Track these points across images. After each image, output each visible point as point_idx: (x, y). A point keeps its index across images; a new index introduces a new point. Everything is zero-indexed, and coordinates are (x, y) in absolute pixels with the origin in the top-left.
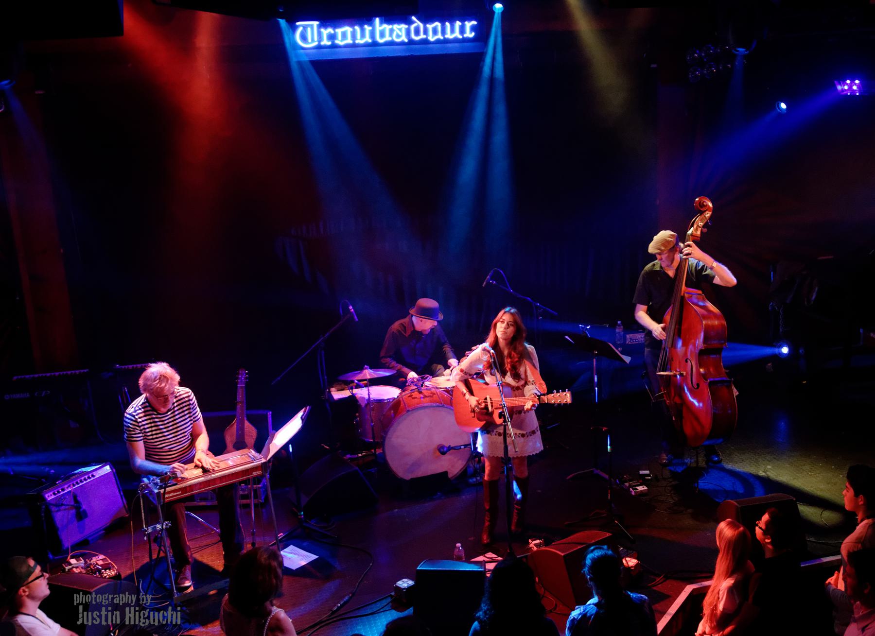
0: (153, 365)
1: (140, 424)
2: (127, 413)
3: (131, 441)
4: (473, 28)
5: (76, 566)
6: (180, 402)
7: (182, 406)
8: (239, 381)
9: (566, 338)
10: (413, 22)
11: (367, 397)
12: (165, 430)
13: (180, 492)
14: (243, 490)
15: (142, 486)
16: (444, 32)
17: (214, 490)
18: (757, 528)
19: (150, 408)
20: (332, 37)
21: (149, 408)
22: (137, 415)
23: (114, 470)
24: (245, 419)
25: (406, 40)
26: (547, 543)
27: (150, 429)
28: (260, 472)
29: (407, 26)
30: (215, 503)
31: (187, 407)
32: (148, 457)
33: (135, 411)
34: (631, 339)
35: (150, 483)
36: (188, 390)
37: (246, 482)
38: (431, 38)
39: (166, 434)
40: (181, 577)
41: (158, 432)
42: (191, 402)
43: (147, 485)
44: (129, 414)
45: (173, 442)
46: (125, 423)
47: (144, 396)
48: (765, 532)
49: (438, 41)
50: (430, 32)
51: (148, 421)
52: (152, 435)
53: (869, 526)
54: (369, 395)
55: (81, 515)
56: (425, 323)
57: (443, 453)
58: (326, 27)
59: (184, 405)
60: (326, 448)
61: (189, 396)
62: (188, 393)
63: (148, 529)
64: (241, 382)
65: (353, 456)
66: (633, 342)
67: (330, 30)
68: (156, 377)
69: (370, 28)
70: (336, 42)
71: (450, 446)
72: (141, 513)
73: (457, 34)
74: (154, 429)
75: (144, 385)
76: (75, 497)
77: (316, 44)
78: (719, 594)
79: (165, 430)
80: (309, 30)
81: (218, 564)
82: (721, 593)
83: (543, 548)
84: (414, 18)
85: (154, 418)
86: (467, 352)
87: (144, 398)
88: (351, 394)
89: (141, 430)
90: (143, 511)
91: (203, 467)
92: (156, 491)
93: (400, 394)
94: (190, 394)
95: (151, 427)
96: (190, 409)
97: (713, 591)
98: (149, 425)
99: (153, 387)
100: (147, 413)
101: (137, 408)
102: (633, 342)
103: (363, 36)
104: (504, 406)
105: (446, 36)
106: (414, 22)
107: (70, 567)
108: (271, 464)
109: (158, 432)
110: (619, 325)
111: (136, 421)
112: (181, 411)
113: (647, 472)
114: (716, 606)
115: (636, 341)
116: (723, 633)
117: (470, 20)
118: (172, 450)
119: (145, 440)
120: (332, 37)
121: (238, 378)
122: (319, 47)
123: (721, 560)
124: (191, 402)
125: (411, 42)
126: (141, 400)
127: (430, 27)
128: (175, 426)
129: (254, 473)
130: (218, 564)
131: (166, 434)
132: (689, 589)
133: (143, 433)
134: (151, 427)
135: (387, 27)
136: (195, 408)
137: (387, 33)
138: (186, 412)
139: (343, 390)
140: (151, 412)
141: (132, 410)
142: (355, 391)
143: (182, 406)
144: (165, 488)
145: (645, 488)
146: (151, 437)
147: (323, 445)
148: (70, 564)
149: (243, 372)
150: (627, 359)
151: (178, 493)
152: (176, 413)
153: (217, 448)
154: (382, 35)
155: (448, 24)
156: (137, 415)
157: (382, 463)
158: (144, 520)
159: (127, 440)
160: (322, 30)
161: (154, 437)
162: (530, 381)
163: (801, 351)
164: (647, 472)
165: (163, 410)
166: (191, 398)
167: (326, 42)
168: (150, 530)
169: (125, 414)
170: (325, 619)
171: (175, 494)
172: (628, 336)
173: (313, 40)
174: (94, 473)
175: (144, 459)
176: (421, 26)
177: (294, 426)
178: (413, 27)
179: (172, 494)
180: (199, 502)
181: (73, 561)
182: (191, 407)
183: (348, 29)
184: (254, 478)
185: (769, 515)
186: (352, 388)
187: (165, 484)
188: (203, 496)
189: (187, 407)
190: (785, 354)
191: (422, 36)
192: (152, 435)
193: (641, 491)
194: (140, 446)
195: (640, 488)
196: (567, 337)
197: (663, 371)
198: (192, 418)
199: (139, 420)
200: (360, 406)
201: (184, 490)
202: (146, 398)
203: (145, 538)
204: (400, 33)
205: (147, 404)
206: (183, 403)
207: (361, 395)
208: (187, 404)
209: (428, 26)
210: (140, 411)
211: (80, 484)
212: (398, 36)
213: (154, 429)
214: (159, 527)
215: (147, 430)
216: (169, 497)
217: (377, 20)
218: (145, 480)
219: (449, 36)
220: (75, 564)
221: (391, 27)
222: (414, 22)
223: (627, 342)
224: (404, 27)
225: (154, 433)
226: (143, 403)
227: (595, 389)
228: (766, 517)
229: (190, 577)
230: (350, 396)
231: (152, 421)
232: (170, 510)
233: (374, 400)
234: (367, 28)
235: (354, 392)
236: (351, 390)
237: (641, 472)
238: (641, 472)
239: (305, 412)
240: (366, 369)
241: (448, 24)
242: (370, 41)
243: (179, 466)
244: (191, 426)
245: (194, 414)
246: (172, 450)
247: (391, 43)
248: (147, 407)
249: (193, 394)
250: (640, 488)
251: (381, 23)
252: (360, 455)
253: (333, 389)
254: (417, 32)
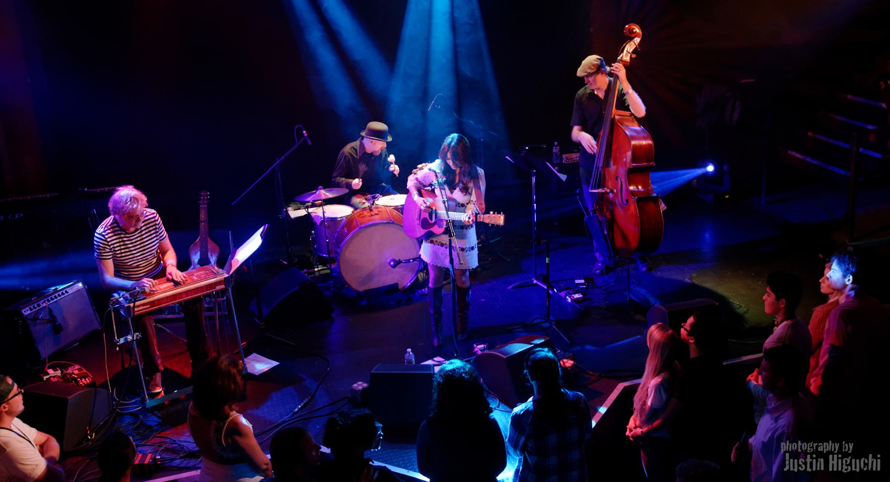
0: (121, 188)
1: (110, 243)
2: (97, 233)
3: (100, 259)
5: (53, 375)
6: (146, 223)
7: (148, 226)
8: (201, 202)
9: (507, 159)
11: (321, 215)
12: (133, 249)
13: (149, 306)
14: (208, 303)
15: (112, 300)
17: (180, 303)
18: (682, 330)
19: (118, 228)
21: (117, 229)
22: (106, 235)
23: (86, 287)
24: (208, 238)
26: (489, 348)
27: (119, 248)
28: (223, 286)
30: (182, 315)
31: (154, 227)
32: (117, 274)
33: (104, 232)
34: (567, 159)
35: (120, 298)
36: (153, 211)
37: (208, 295)
39: (134, 252)
40: (152, 384)
41: (127, 250)
42: (157, 223)
43: (117, 300)
44: (99, 234)
45: (140, 260)
46: (95, 243)
47: (112, 217)
48: (690, 333)
51: (117, 241)
52: (121, 253)
53: (789, 327)
54: (324, 215)
55: (57, 329)
56: (375, 144)
57: (394, 267)
59: (151, 225)
60: (285, 264)
61: (155, 217)
62: (153, 214)
63: (120, 340)
64: (204, 204)
65: (310, 271)
66: (569, 161)
68: (127, 200)
71: (400, 260)
72: (113, 325)
74: (122, 247)
75: (114, 207)
76: (50, 311)
78: (647, 391)
79: (133, 249)
81: (187, 371)
82: (649, 390)
83: (486, 352)
85: (123, 238)
86: (414, 170)
87: (112, 219)
88: (307, 213)
89: (111, 249)
90: (114, 324)
91: (173, 280)
92: (126, 305)
93: (352, 212)
94: (155, 215)
95: (120, 246)
96: (156, 229)
97: (642, 388)
98: (118, 244)
99: (126, 209)
100: (116, 233)
101: (106, 229)
102: (569, 161)
104: (450, 222)
107: (48, 377)
108: (233, 279)
109: (127, 250)
110: (556, 146)
111: (106, 241)
112: (147, 230)
113: (583, 281)
114: (645, 403)
115: (571, 161)
116: (652, 426)
118: (140, 266)
119: (115, 258)
121: (200, 200)
123: (651, 358)
124: (157, 223)
126: (109, 220)
128: (142, 245)
129: (217, 287)
130: (187, 371)
131: (134, 252)
132: (621, 386)
133: (112, 252)
134: (120, 246)
136: (161, 227)
138: (152, 232)
139: (299, 209)
140: (119, 232)
141: (102, 230)
142: (310, 210)
143: (148, 226)
144: (134, 302)
145: (581, 296)
146: (120, 255)
147: (281, 260)
148: (48, 374)
149: (205, 194)
150: (563, 177)
151: (147, 307)
152: (144, 232)
153: (183, 264)
156: (106, 235)
157: (336, 278)
158: (115, 332)
159: (97, 258)
161: (123, 255)
162: (472, 201)
163: (725, 168)
164: (583, 281)
165: (132, 229)
166: (156, 218)
168: (122, 341)
169: (96, 234)
170: (287, 420)
171: (144, 307)
172: (564, 156)
174: (67, 290)
175: (113, 275)
177: (255, 243)
179: (141, 308)
180: (166, 315)
181: (51, 371)
182: (158, 226)
184: (217, 292)
185: (694, 319)
186: (307, 207)
187: (135, 299)
188: (170, 309)
189: (154, 227)
190: (712, 172)
192: (121, 253)
193: (577, 298)
194: (109, 265)
195: (577, 296)
196: (507, 157)
197: (594, 189)
198: (158, 237)
199: (109, 240)
200: (315, 223)
201: (152, 303)
202: (115, 219)
203: (117, 349)
205: (115, 225)
206: (150, 223)
207: (316, 213)
208: (152, 224)
210: (109, 231)
211: (55, 300)
213: (122, 247)
214: (130, 338)
215: (117, 249)
216: (138, 311)
218: (116, 295)
220: (53, 373)
223: (564, 161)
225: (123, 251)
226: (112, 224)
227: (534, 206)
228: (691, 320)
229: (161, 385)
230: (306, 215)
231: (120, 240)
232: (139, 322)
233: (328, 218)
235: (309, 211)
236: (306, 209)
237: (577, 281)
238: (577, 281)
239: (265, 227)
240: (321, 189)
243: (148, 281)
244: (158, 244)
245: (160, 234)
246: (140, 266)
248: (115, 227)
249: (158, 215)
250: (577, 296)
252: (316, 269)
253: (290, 209)
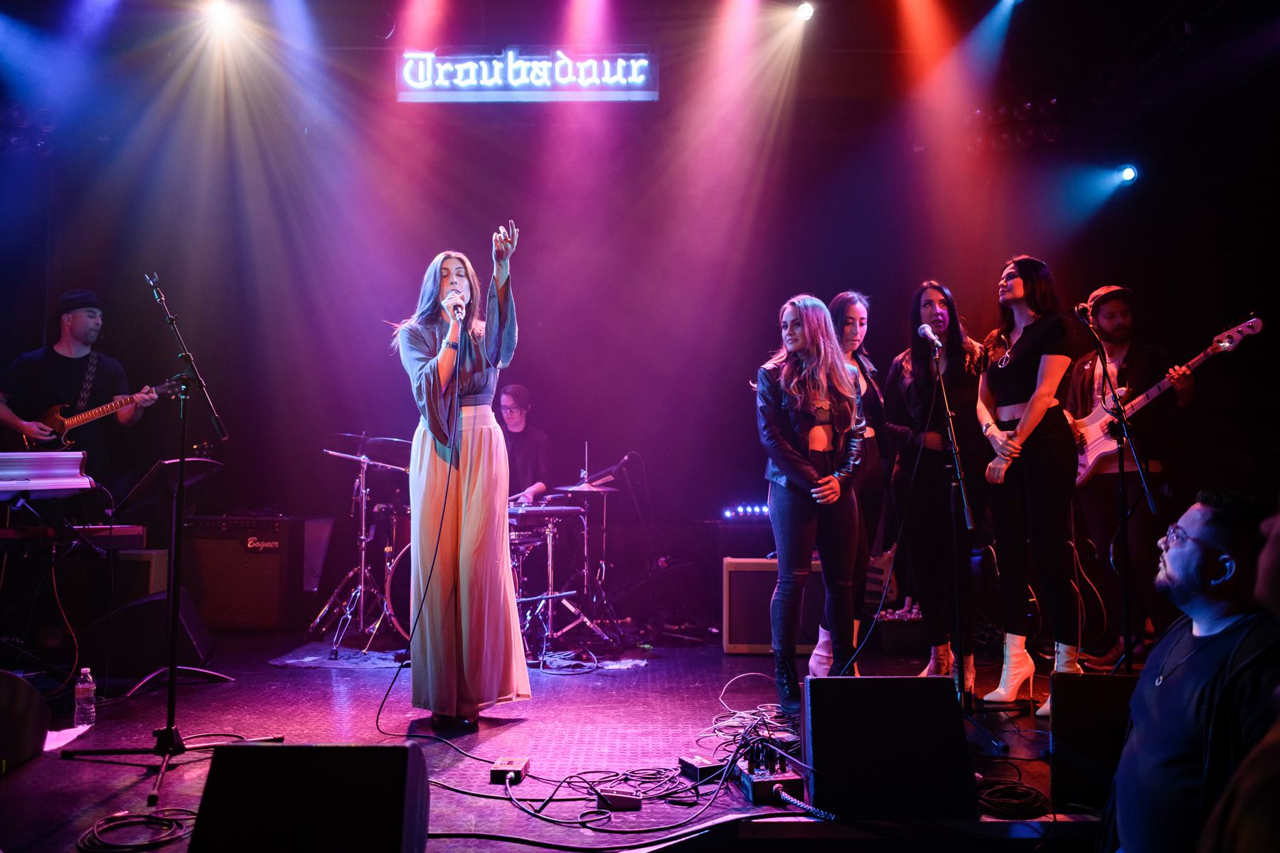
4: (641, 71)
10: (559, 59)
16: (601, 73)
20: (451, 76)
25: (549, 83)
29: (549, 64)
38: (584, 82)
49: (593, 88)
58: (444, 62)
67: (448, 67)
73: (620, 78)
80: (421, 64)
103: (491, 75)
106: (561, 59)
117: (638, 58)
120: (451, 76)
122: (436, 89)
125: (555, 87)
127: (582, 66)
135: (523, 64)
137: (523, 73)
154: (517, 74)
160: (438, 65)
167: (443, 82)
176: (569, 62)
178: (558, 65)
183: (471, 66)
191: (570, 78)
204: (540, 73)
209: (579, 64)
212: (538, 77)
217: (511, 54)
219: (609, 80)
221: (528, 64)
222: (561, 59)
224: (546, 65)
234: (497, 65)
241: (606, 63)
242: (500, 82)
247: (529, 88)
251: (516, 59)
254: (564, 72)
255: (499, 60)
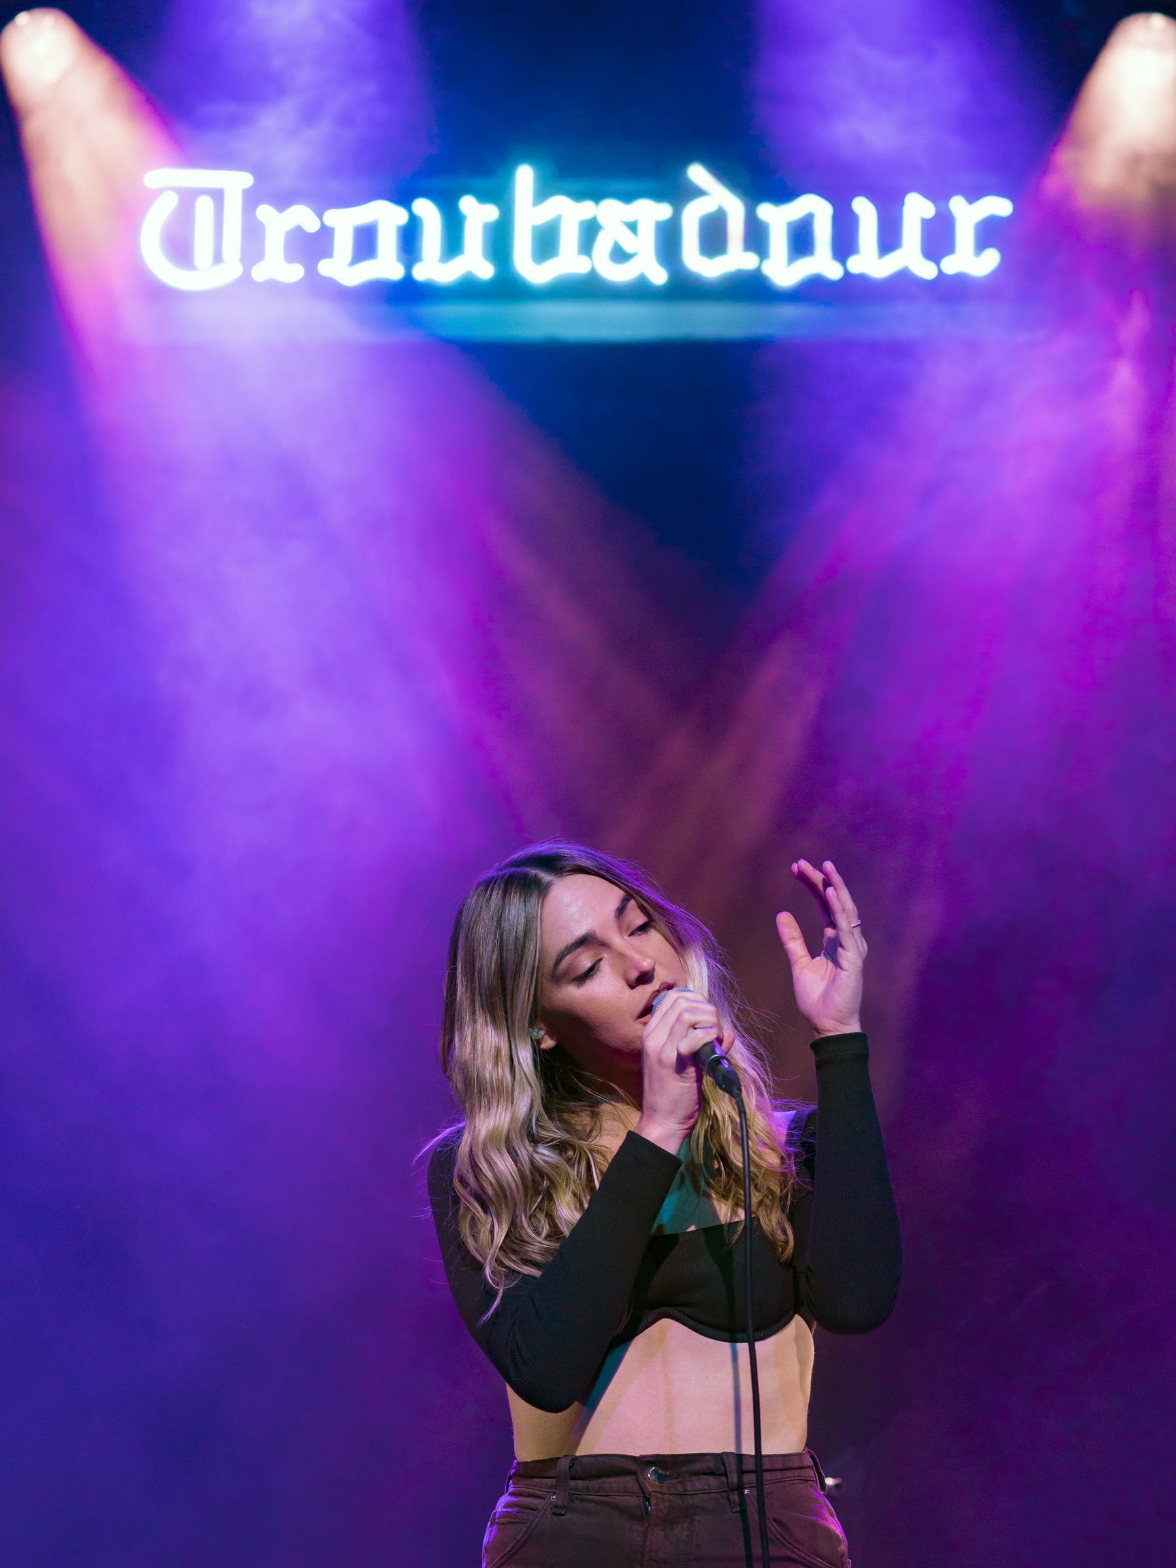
4: (989, 233)
10: (697, 192)
16: (844, 245)
25: (659, 276)
29: (664, 211)
50: (779, 241)
58: (282, 201)
67: (303, 217)
69: (491, 212)
70: (325, 268)
77: (231, 270)
84: (697, 173)
103: (453, 244)
105: (856, 265)
117: (973, 196)
137: (569, 238)
155: (864, 208)
160: (265, 212)
173: (218, 258)
176: (734, 207)
178: (693, 214)
209: (766, 211)
212: (620, 255)
217: (525, 176)
221: (587, 209)
222: (698, 192)
241: (864, 208)
242: (485, 271)
251: (542, 193)
255: (484, 197)
